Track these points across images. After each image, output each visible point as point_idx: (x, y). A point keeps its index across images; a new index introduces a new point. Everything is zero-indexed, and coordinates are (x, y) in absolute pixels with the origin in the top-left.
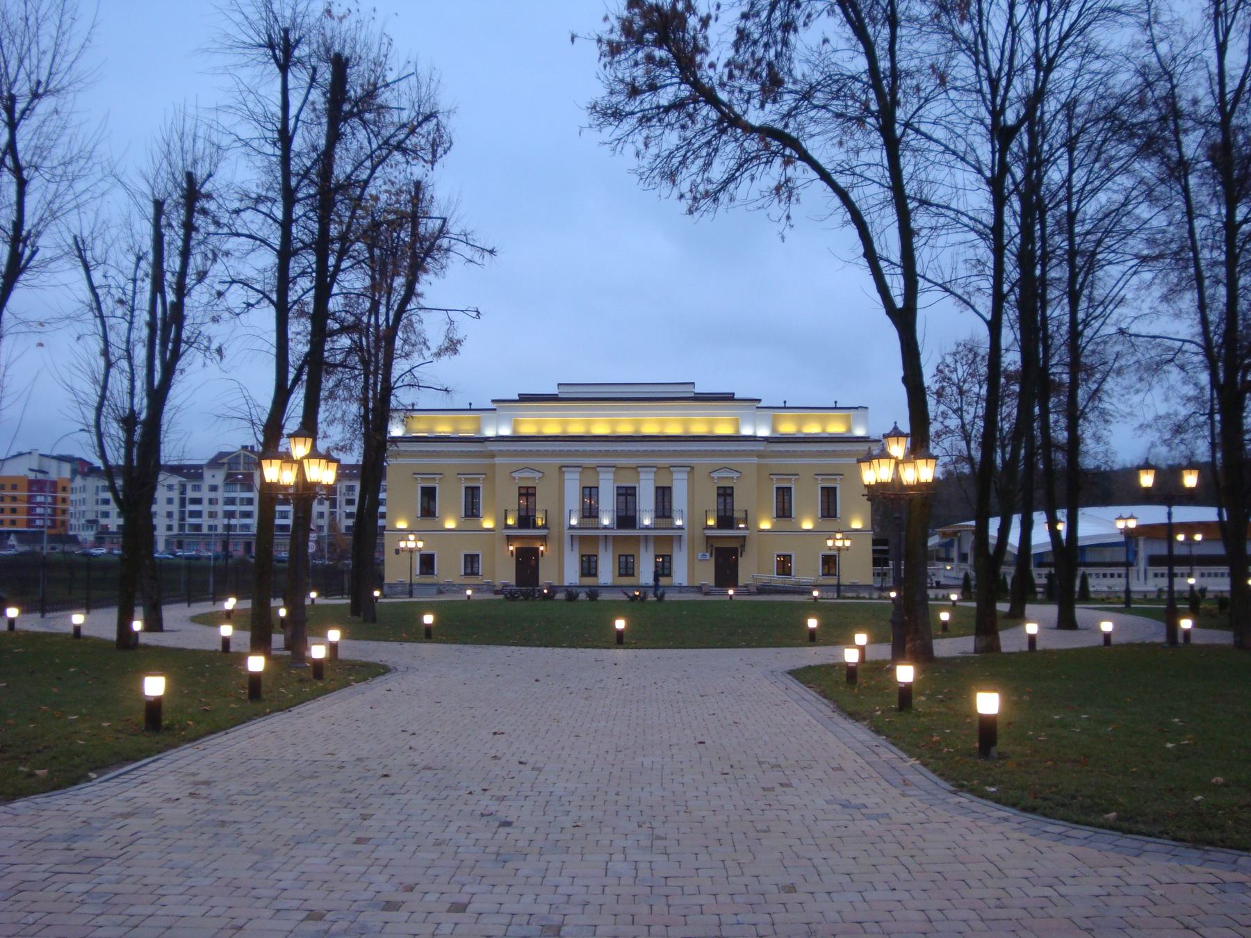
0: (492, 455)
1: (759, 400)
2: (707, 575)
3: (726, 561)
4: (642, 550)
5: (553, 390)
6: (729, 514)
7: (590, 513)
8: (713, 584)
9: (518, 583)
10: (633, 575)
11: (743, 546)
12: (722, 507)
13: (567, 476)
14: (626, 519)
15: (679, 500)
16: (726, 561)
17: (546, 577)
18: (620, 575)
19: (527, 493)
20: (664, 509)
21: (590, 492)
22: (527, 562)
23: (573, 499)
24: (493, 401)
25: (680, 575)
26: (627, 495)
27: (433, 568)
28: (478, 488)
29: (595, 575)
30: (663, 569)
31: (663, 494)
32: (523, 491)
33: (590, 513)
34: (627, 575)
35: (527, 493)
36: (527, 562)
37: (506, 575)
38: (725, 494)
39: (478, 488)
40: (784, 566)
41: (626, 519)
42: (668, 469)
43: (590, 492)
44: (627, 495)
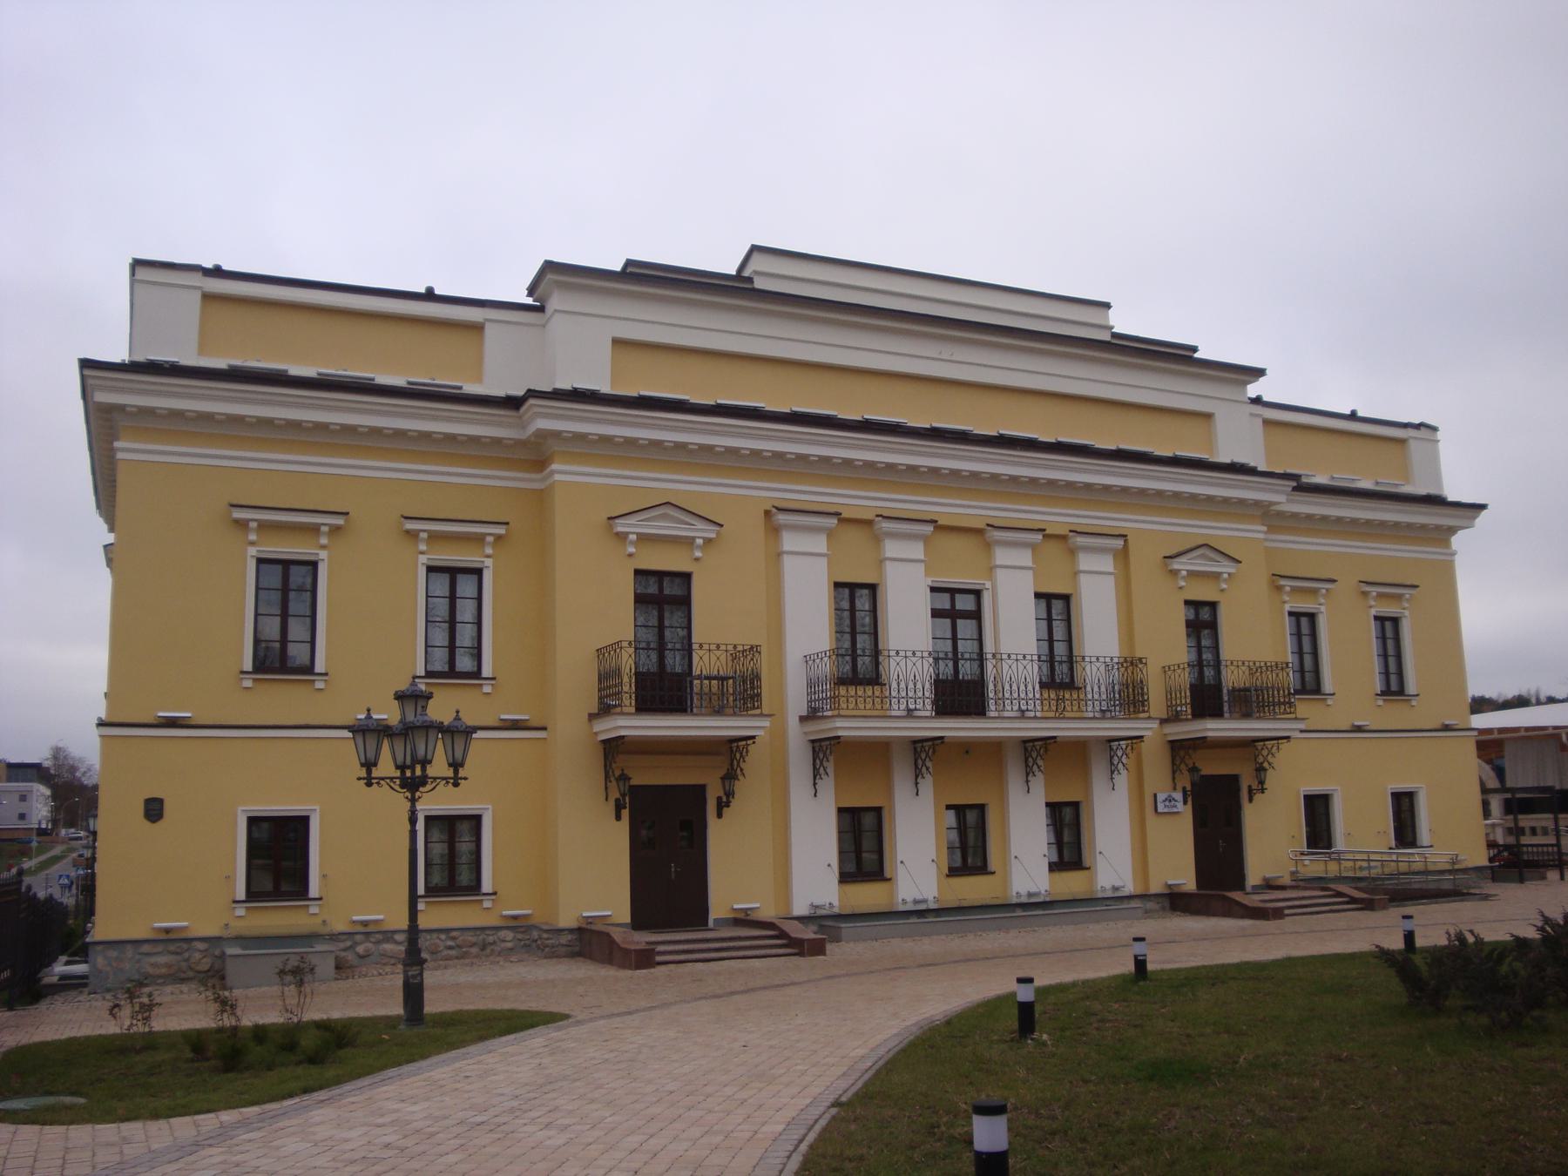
6: (967, 670)
7: (858, 662)
10: (982, 869)
12: (1045, 650)
13: (790, 541)
14: (960, 694)
15: (1099, 638)
17: (734, 879)
19: (664, 596)
21: (857, 603)
23: (809, 630)
25: (1113, 862)
26: (958, 609)
31: (1056, 607)
33: (858, 662)
35: (664, 596)
41: (960, 694)
42: (1063, 541)
43: (857, 603)
44: (958, 609)
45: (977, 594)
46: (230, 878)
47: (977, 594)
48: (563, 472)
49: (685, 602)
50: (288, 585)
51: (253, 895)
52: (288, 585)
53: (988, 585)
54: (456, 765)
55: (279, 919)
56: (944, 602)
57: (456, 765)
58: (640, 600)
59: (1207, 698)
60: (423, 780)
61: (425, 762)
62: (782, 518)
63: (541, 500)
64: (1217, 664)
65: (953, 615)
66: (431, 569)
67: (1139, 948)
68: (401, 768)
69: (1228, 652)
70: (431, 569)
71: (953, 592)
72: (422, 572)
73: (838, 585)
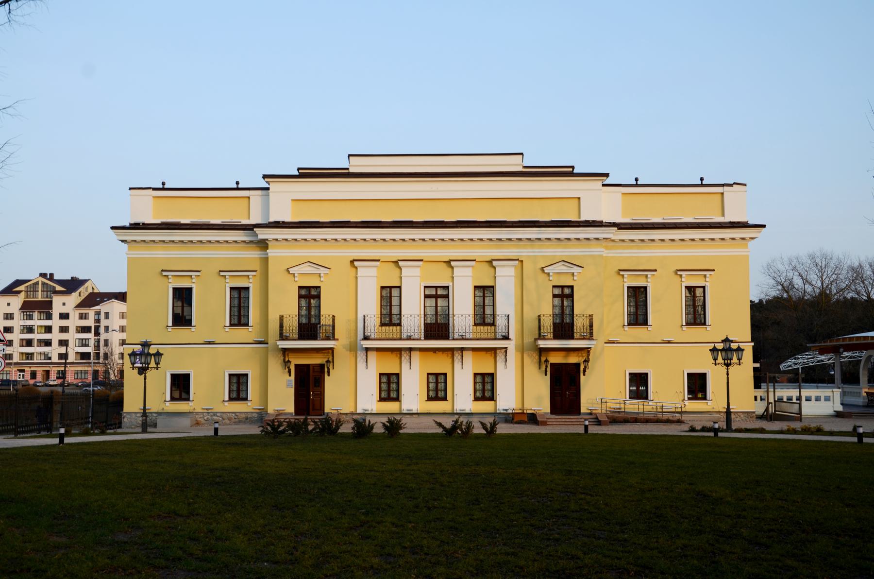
0: (263, 245)
1: (607, 175)
2: (539, 397)
3: (565, 383)
4: (457, 365)
5: (339, 162)
6: (567, 320)
7: (390, 318)
8: (549, 411)
9: (299, 409)
10: (445, 399)
11: (587, 361)
14: (438, 329)
15: (505, 305)
16: (565, 383)
18: (430, 399)
19: (310, 295)
20: (484, 318)
22: (309, 383)
23: (370, 306)
24: (265, 177)
26: (438, 294)
27: (188, 393)
28: (247, 289)
29: (397, 399)
30: (485, 387)
31: (485, 292)
32: (303, 292)
33: (390, 318)
34: (436, 398)
35: (310, 295)
36: (309, 383)
37: (282, 399)
38: (565, 295)
39: (247, 289)
40: (639, 383)
41: (438, 329)
43: (389, 296)
44: (438, 294)
45: (447, 287)
46: (164, 393)
47: (572, 287)
48: (271, 252)
49: (318, 297)
50: (183, 296)
51: (173, 399)
52: (183, 296)
53: (451, 284)
54: (739, 359)
55: (181, 407)
56: (557, 291)
57: (739, 359)
58: (300, 297)
59: (564, 328)
60: (730, 364)
61: (731, 359)
62: (356, 263)
63: (265, 261)
64: (319, 316)
65: (562, 296)
66: (231, 289)
67: (217, 425)
68: (724, 360)
69: (324, 311)
70: (231, 289)
71: (563, 287)
72: (228, 290)
73: (476, 287)
